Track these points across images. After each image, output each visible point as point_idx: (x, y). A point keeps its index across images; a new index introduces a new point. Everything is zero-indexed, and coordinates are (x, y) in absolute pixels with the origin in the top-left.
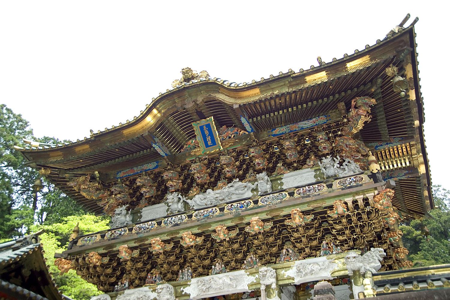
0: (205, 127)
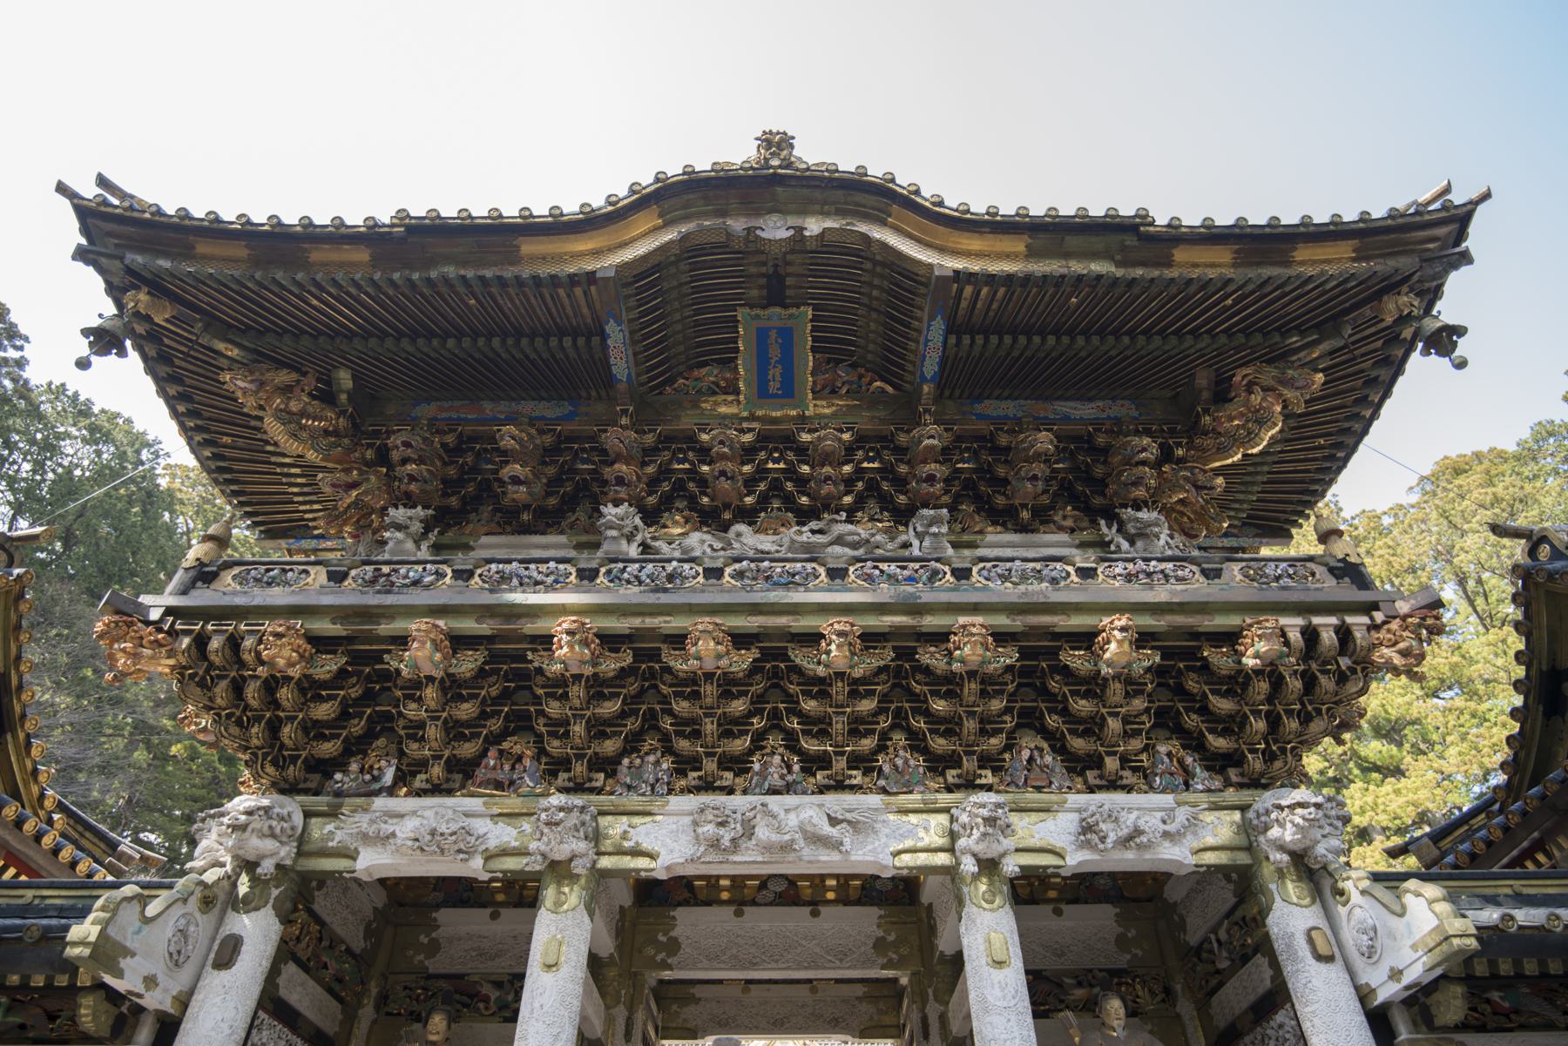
0: (773, 334)
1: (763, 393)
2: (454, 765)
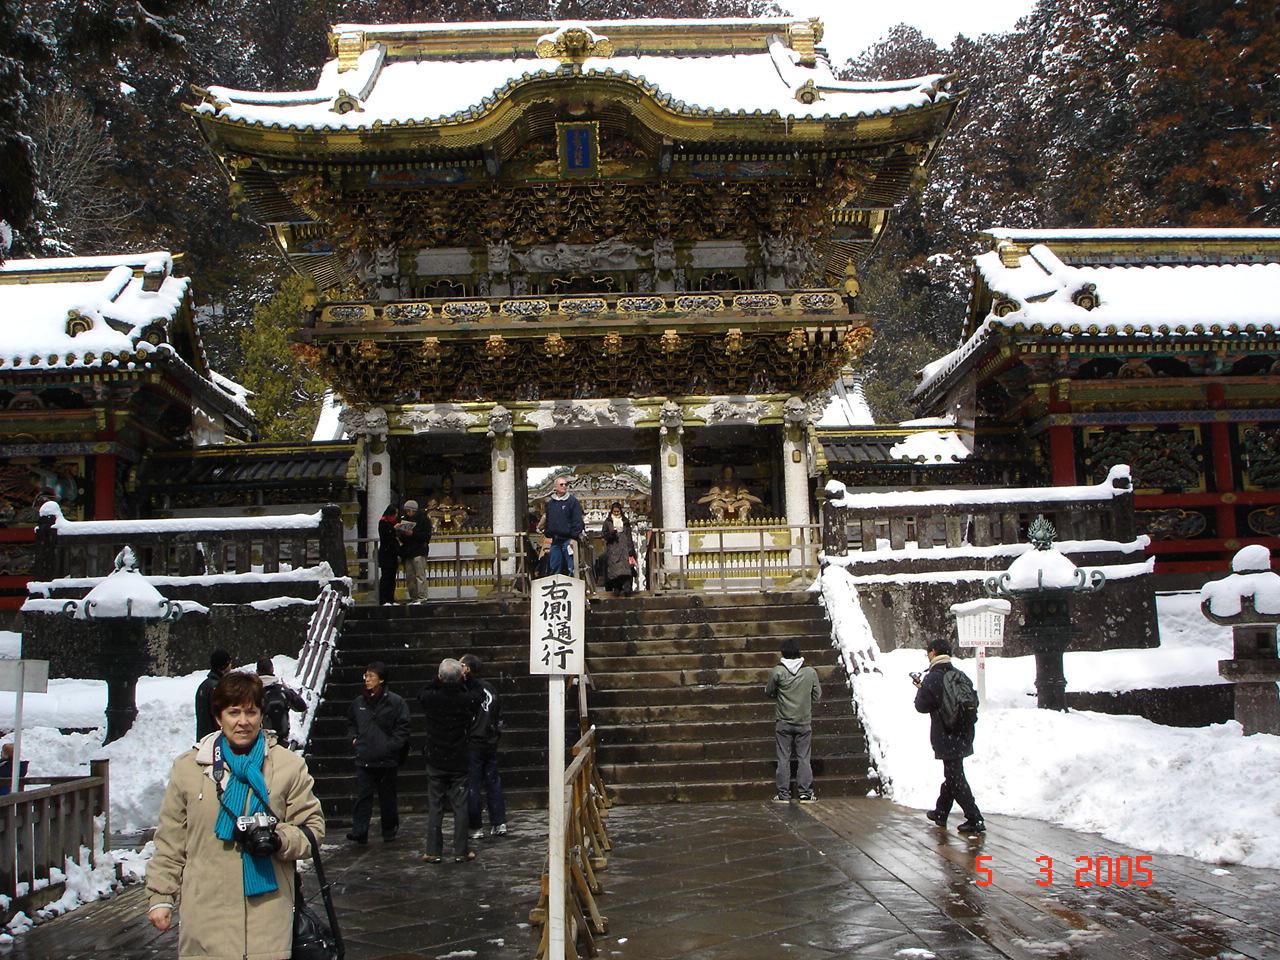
1: (571, 165)
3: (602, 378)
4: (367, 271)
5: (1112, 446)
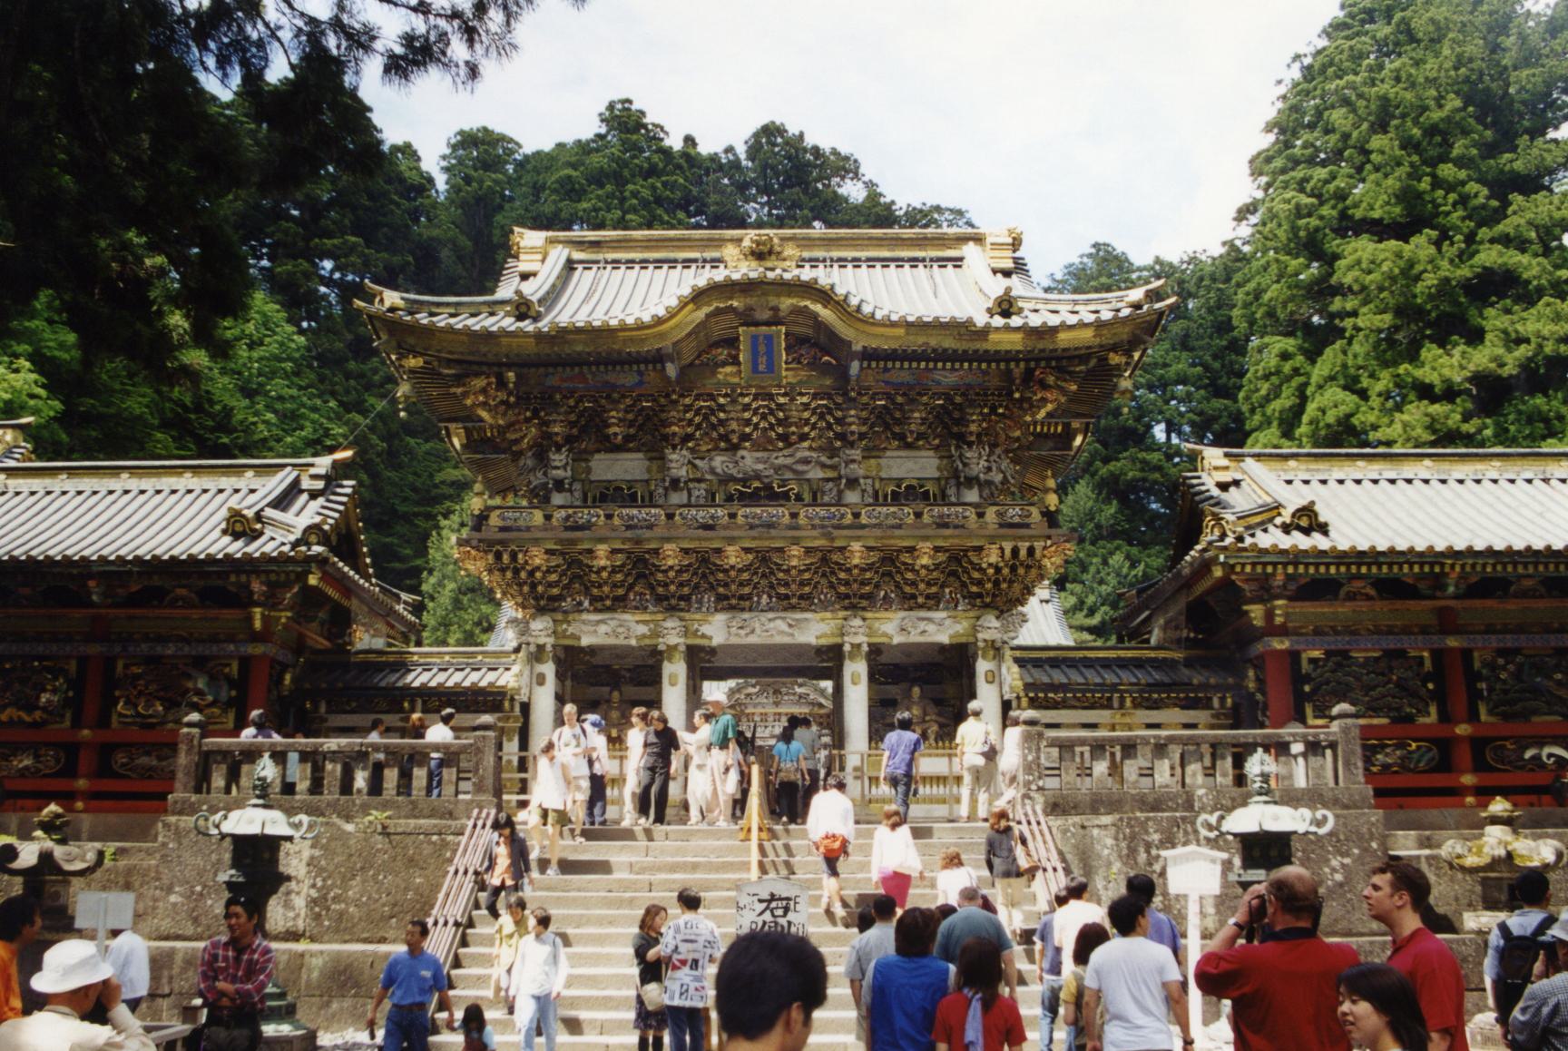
1: (755, 370)
2: (616, 599)
3: (782, 590)
4: (539, 474)
5: (1333, 671)
